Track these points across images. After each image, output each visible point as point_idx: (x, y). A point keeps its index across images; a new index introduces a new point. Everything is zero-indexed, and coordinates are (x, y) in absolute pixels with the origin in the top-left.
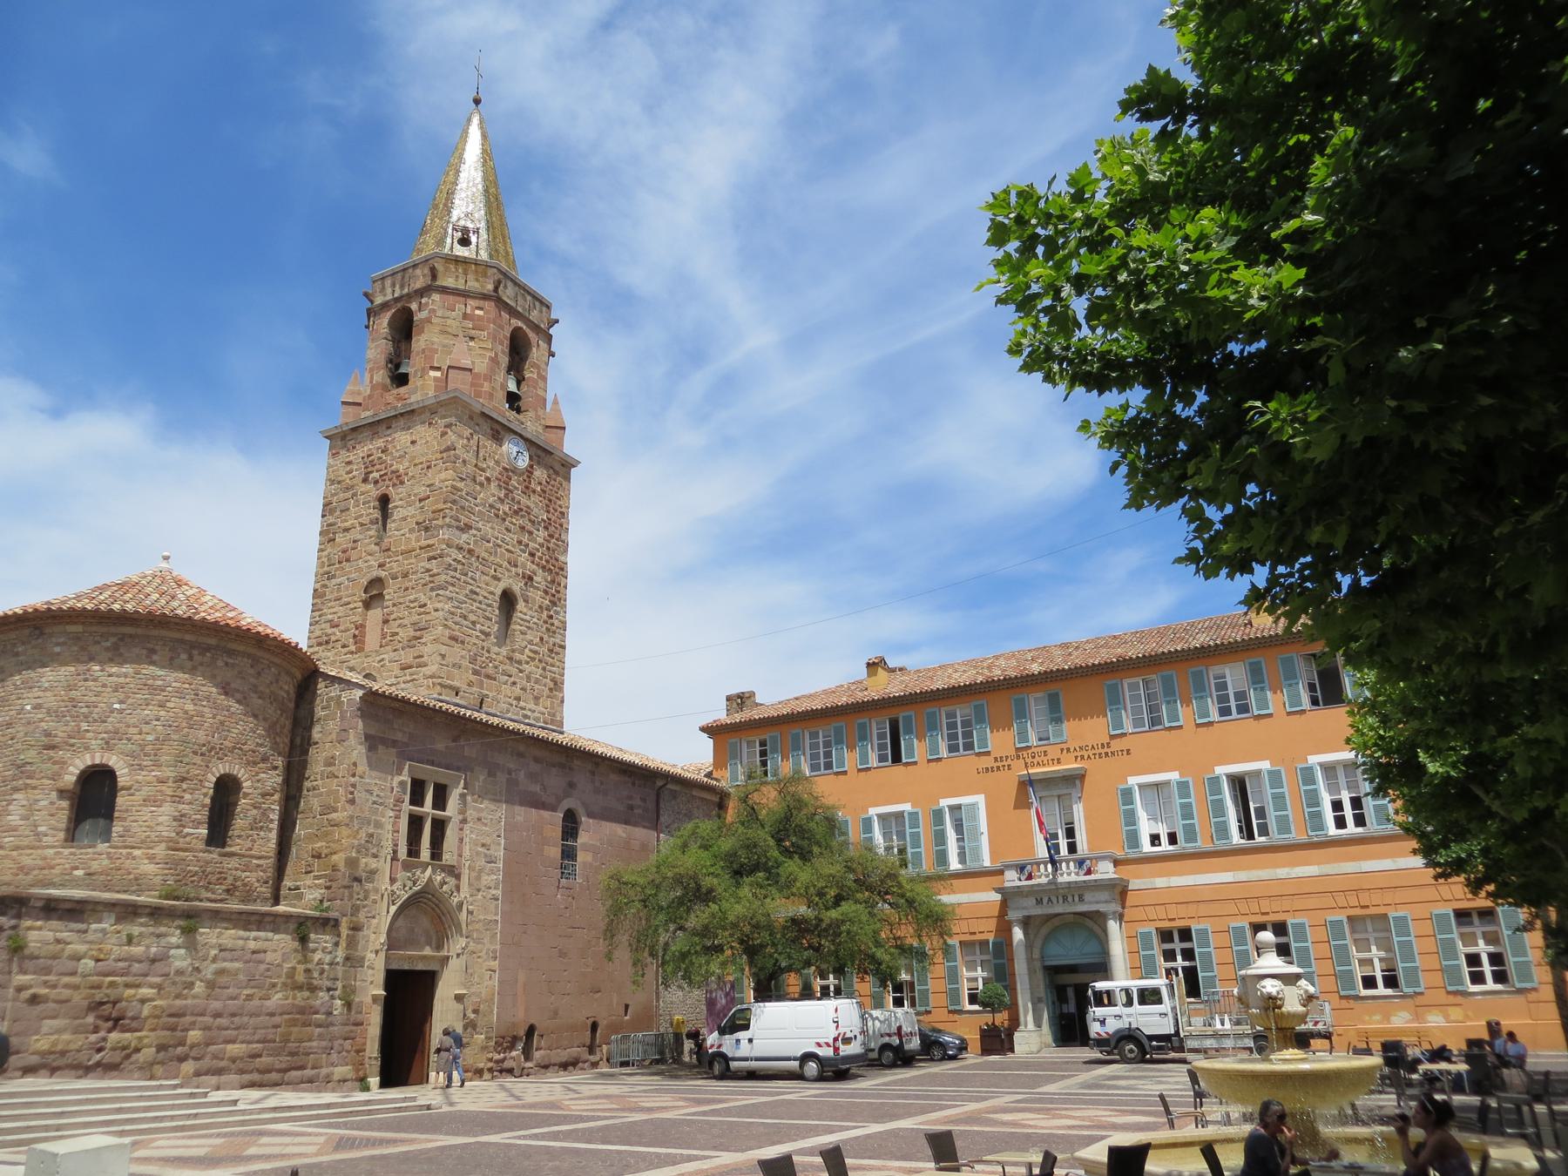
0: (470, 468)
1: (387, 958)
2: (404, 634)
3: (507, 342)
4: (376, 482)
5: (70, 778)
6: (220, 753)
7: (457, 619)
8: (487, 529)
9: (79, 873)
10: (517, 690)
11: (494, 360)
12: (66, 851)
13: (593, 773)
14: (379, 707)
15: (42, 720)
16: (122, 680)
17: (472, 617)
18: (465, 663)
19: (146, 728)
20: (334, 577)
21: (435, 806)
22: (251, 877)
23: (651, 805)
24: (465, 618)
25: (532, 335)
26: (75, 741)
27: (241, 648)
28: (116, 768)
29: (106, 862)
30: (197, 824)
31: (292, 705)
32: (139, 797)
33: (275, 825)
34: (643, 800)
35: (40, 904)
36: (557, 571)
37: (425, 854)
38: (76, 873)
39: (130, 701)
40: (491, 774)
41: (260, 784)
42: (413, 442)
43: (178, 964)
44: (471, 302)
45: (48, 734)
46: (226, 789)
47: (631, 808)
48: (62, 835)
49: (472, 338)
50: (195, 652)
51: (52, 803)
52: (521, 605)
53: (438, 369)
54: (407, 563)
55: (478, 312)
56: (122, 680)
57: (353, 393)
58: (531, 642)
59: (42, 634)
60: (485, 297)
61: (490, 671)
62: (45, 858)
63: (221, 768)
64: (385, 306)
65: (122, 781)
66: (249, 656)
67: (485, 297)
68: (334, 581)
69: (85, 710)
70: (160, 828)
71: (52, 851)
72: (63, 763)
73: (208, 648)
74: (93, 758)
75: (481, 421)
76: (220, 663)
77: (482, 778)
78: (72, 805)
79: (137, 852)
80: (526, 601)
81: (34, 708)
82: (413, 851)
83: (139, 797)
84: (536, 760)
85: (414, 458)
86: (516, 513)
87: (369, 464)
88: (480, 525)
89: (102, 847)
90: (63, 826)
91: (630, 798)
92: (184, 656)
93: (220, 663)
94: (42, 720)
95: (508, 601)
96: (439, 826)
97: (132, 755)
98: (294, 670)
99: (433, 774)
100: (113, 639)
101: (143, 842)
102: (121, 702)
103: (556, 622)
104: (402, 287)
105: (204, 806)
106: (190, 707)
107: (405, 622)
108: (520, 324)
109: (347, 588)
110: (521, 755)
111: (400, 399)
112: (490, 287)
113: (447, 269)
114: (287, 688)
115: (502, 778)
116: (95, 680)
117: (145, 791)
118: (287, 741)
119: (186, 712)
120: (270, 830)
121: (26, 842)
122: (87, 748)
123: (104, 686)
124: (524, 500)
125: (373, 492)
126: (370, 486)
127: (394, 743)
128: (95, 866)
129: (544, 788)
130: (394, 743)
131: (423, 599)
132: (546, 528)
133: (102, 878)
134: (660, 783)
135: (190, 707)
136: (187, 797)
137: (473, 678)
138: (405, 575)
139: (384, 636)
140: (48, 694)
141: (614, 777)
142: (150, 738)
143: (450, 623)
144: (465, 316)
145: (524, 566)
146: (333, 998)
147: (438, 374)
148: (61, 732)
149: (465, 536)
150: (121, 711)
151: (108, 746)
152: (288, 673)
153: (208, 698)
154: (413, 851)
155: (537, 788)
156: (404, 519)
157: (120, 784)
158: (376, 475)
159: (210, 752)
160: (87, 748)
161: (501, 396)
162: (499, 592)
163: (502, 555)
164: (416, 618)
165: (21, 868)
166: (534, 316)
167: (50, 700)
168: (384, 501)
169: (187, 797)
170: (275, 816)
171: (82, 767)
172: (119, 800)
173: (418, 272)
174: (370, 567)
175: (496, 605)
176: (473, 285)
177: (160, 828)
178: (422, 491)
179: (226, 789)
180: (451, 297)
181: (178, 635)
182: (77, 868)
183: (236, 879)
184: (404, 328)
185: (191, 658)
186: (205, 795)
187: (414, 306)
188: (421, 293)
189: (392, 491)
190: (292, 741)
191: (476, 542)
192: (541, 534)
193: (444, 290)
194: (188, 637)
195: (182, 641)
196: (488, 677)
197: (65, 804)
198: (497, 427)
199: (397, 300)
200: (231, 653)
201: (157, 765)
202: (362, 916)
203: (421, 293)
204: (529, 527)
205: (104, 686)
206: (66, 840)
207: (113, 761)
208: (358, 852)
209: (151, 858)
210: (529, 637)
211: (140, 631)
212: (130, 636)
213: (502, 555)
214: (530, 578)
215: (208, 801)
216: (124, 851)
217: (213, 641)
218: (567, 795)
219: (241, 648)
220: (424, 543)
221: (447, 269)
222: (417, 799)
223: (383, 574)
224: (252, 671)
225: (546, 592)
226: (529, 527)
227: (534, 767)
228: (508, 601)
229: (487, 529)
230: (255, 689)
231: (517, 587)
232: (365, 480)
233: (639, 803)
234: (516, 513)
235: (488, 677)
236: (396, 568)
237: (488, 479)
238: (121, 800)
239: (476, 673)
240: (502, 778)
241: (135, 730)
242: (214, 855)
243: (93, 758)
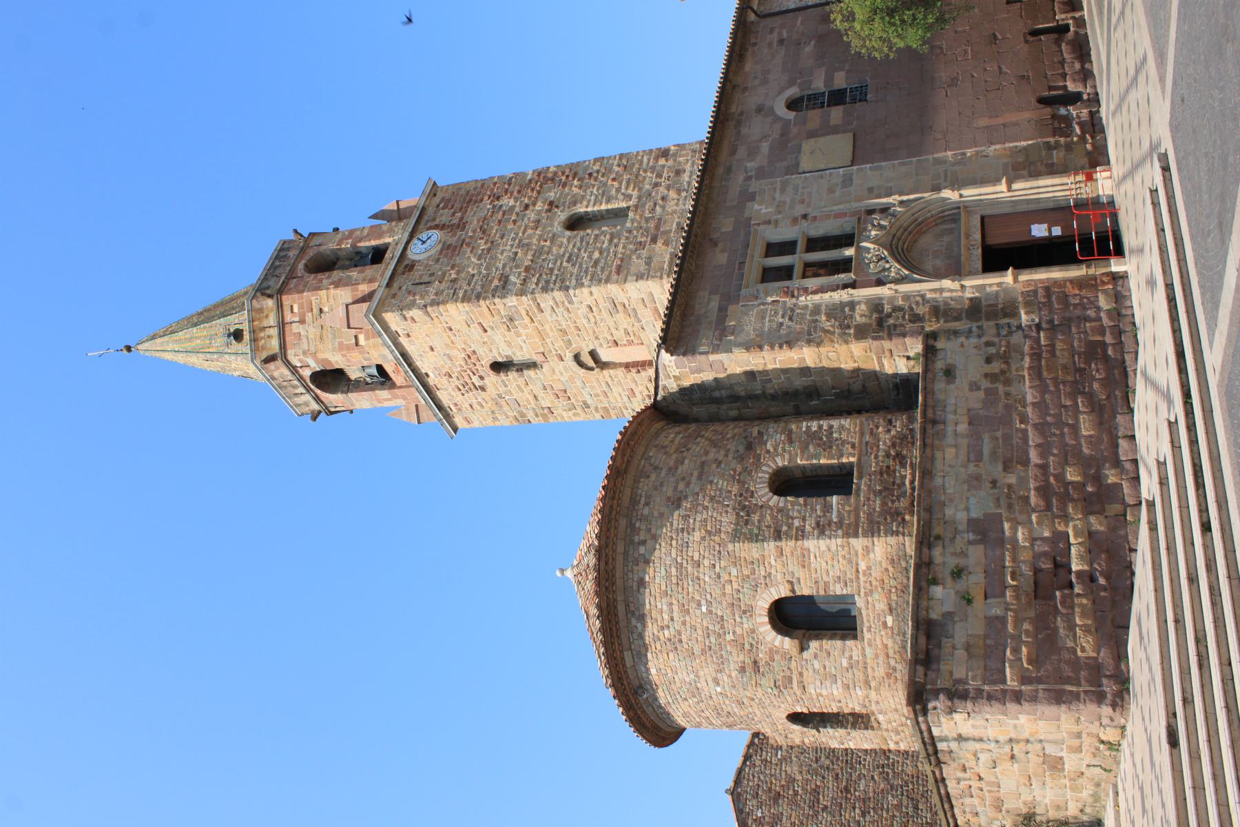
1: (971, 274)
2: (623, 321)
3: (320, 276)
4: (482, 378)
5: (787, 644)
8: (502, 258)
9: (890, 620)
10: (673, 194)
11: (337, 285)
12: (867, 636)
13: (745, 89)
14: (678, 333)
15: (730, 676)
16: (675, 608)
17: (596, 255)
18: (644, 253)
19: (725, 577)
20: (585, 403)
21: (793, 252)
22: (885, 438)
23: (776, 22)
24: (596, 262)
25: (311, 253)
26: (747, 645)
27: (628, 491)
28: (771, 601)
29: (876, 596)
30: (827, 508)
31: (693, 426)
32: (800, 573)
33: (825, 424)
34: (772, 30)
35: (920, 669)
36: (544, 178)
37: (849, 252)
38: (890, 623)
39: (697, 597)
40: (752, 197)
41: (783, 450)
42: (432, 349)
44: (288, 317)
45: (742, 670)
46: (785, 484)
47: (781, 42)
48: (849, 643)
49: (321, 310)
50: (636, 539)
51: (816, 656)
52: (581, 209)
53: (356, 337)
54: (553, 337)
55: (296, 310)
56: (675, 608)
57: (408, 414)
58: (618, 190)
59: (641, 687)
60: (280, 306)
61: (652, 225)
62: (877, 656)
63: (763, 493)
64: (317, 399)
65: (784, 592)
66: (636, 481)
67: (280, 306)
68: (589, 402)
69: (713, 639)
70: (833, 548)
71: (868, 650)
72: (772, 652)
73: (631, 526)
74: (762, 624)
75: (396, 285)
76: (646, 511)
77: (756, 207)
78: (817, 637)
79: (863, 566)
80: (575, 203)
81: (718, 684)
82: (844, 265)
83: (800, 573)
84: (733, 152)
85: (447, 345)
86: (484, 232)
87: (465, 388)
88: (501, 266)
89: (860, 602)
90: (839, 643)
91: (770, 45)
92: (642, 550)
93: (646, 511)
94: (730, 676)
95: (575, 223)
96: (814, 244)
97: (755, 588)
98: (653, 430)
99: (757, 260)
100: (634, 621)
101: (850, 561)
102: (699, 605)
103: (596, 168)
104: (295, 387)
105: (805, 505)
106: (697, 535)
107: (611, 324)
108: (301, 266)
109: (593, 387)
110: (729, 170)
111: (397, 371)
112: (270, 303)
113: (264, 348)
114: (672, 436)
115: (754, 186)
116: (680, 634)
117: (793, 566)
118: (732, 425)
119: (703, 538)
120: (831, 427)
121: (860, 675)
122: (753, 631)
123: (684, 623)
125: (492, 379)
126: (487, 381)
127: (723, 310)
128: (881, 606)
129: (765, 137)
130: (723, 310)
131: (584, 310)
133: (894, 597)
134: (752, 17)
136: (797, 523)
138: (564, 332)
139: (630, 343)
140: (701, 673)
141: (748, 66)
142: (734, 572)
143: (604, 277)
144: (302, 322)
145: (539, 212)
146: (1019, 327)
147: (361, 338)
148: (736, 658)
149: (513, 278)
150: (709, 603)
151: (748, 612)
152: (657, 435)
153: (686, 518)
154: (844, 265)
155: (765, 147)
156: (509, 344)
157: (789, 594)
158: (475, 379)
159: (745, 510)
160: (753, 631)
162: (568, 233)
163: (530, 237)
164: (605, 315)
165: (889, 675)
166: (292, 254)
167: (708, 672)
168: (497, 367)
169: (797, 523)
170: (814, 426)
171: (774, 633)
172: (806, 592)
173: (276, 374)
174: (565, 368)
175: (582, 233)
176: (272, 320)
177: (833, 548)
178: (476, 331)
179: (785, 484)
180: (288, 339)
181: (620, 559)
182: (885, 624)
183: (888, 455)
184: (330, 379)
185: (644, 542)
186: (793, 504)
187: (307, 373)
188: (294, 370)
189: (487, 361)
190: (735, 419)
191: (517, 267)
192: (507, 202)
193: (283, 346)
194: (620, 548)
195: (626, 554)
196: (657, 227)
197: (814, 644)
198: (401, 268)
199: (308, 390)
200: (634, 501)
201: (762, 560)
202: (921, 310)
203: (294, 370)
205: (684, 623)
206: (855, 637)
207: (764, 602)
208: (848, 327)
209: (867, 550)
210: (613, 192)
211: (620, 598)
212: (627, 605)
213: (530, 237)
214: (551, 203)
215: (801, 500)
216: (862, 579)
217: (623, 522)
218: (771, 111)
219: (628, 491)
220: (527, 320)
221: (264, 348)
222: (785, 273)
223: (569, 356)
224: (653, 477)
225: (564, 185)
227: (742, 152)
228: (575, 223)
229: (502, 258)
230: (672, 470)
231: (562, 215)
232: (483, 389)
233: (775, 34)
236: (560, 344)
238: (805, 590)
239: (654, 240)
240: (754, 186)
241: (728, 587)
242: (861, 484)
243: (762, 624)
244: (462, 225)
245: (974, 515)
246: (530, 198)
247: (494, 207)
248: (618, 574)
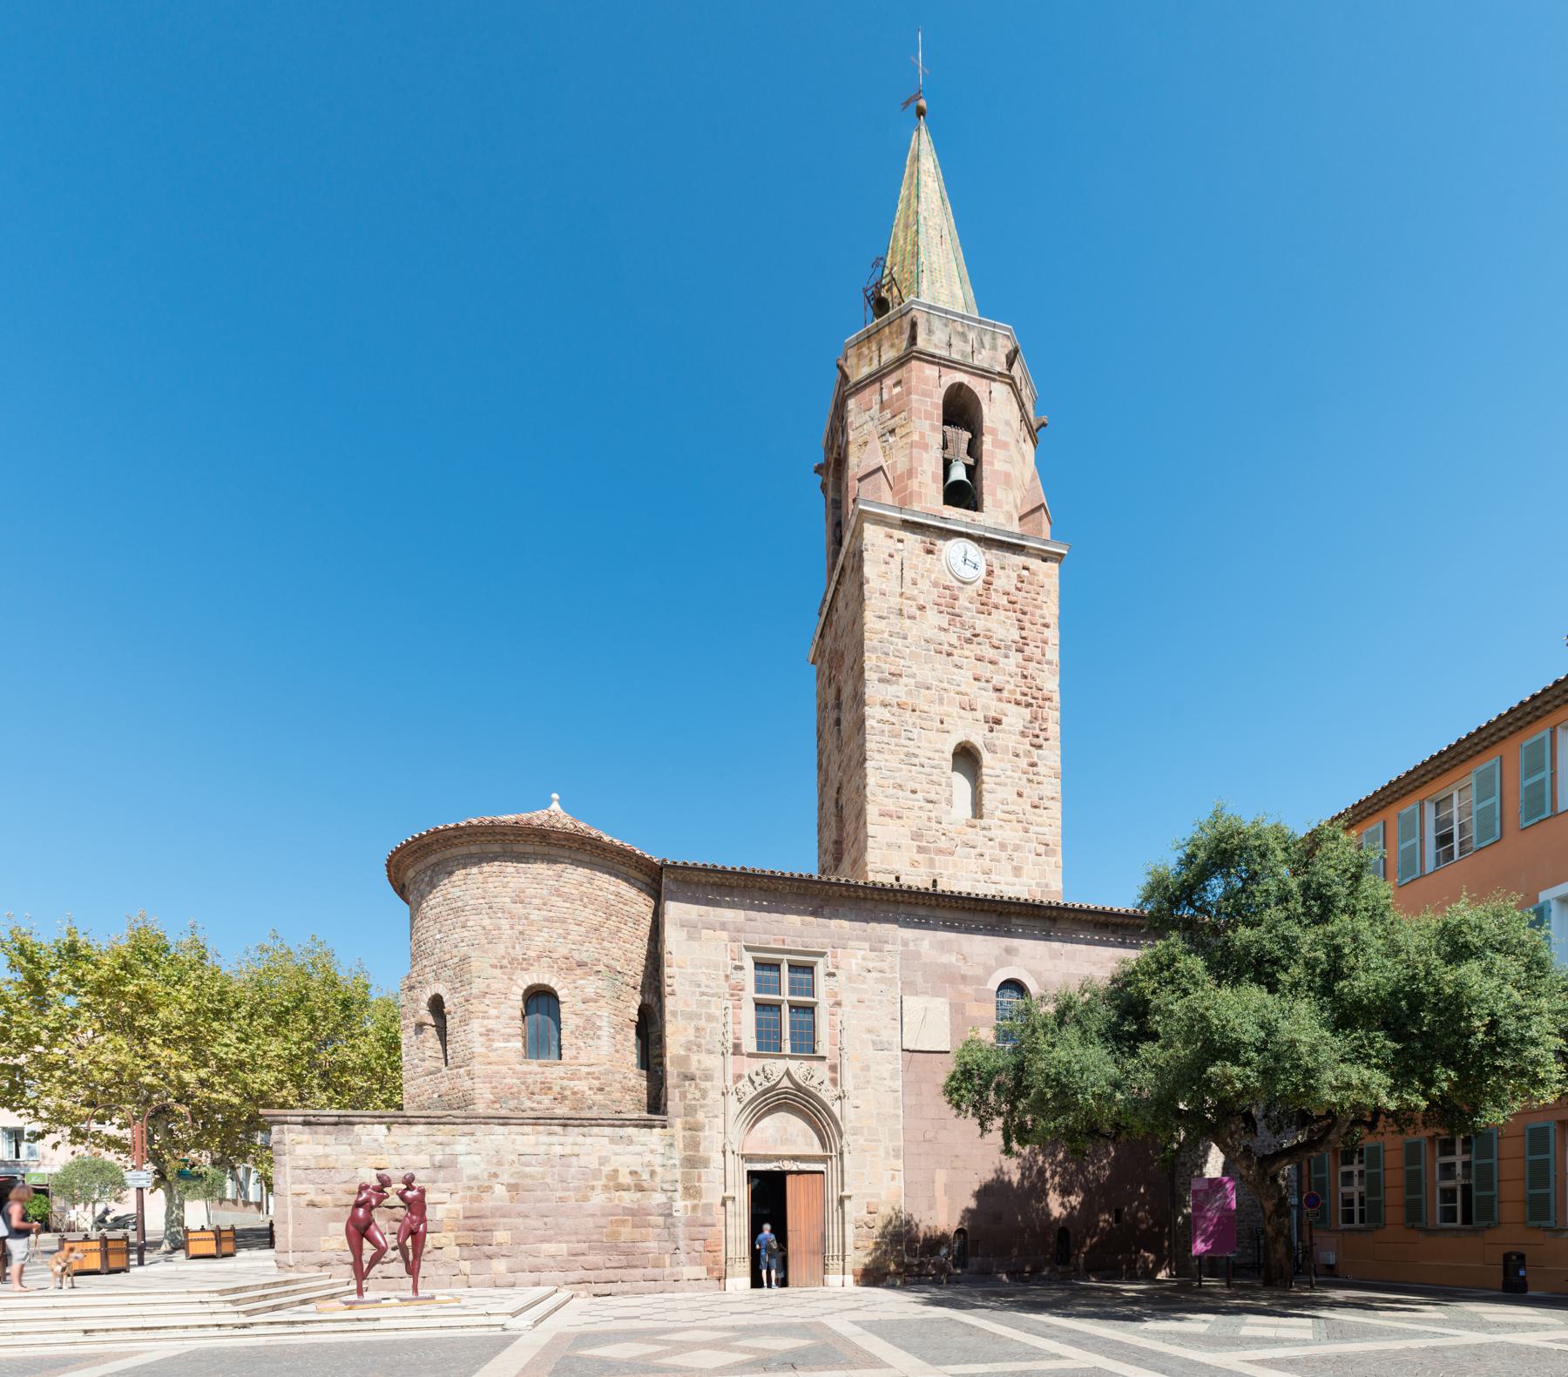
0: (895, 601)
6: (525, 963)
7: (891, 791)
43: (469, 1171)
52: (986, 758)
55: (897, 390)
88: (914, 669)
95: (967, 758)
124: (981, 623)
132: (1020, 650)
135: (486, 922)
137: (920, 857)
161: (935, 492)
162: (950, 748)
181: (464, 850)
196: (940, 852)
204: (990, 653)
214: (998, 722)
225: (1023, 734)
226: (990, 653)
231: (977, 738)
234: (968, 641)
235: (940, 852)
237: (922, 608)
244: (985, 607)
245: (461, 1159)
246: (1012, 692)
247: (1007, 647)
248: (455, 851)
